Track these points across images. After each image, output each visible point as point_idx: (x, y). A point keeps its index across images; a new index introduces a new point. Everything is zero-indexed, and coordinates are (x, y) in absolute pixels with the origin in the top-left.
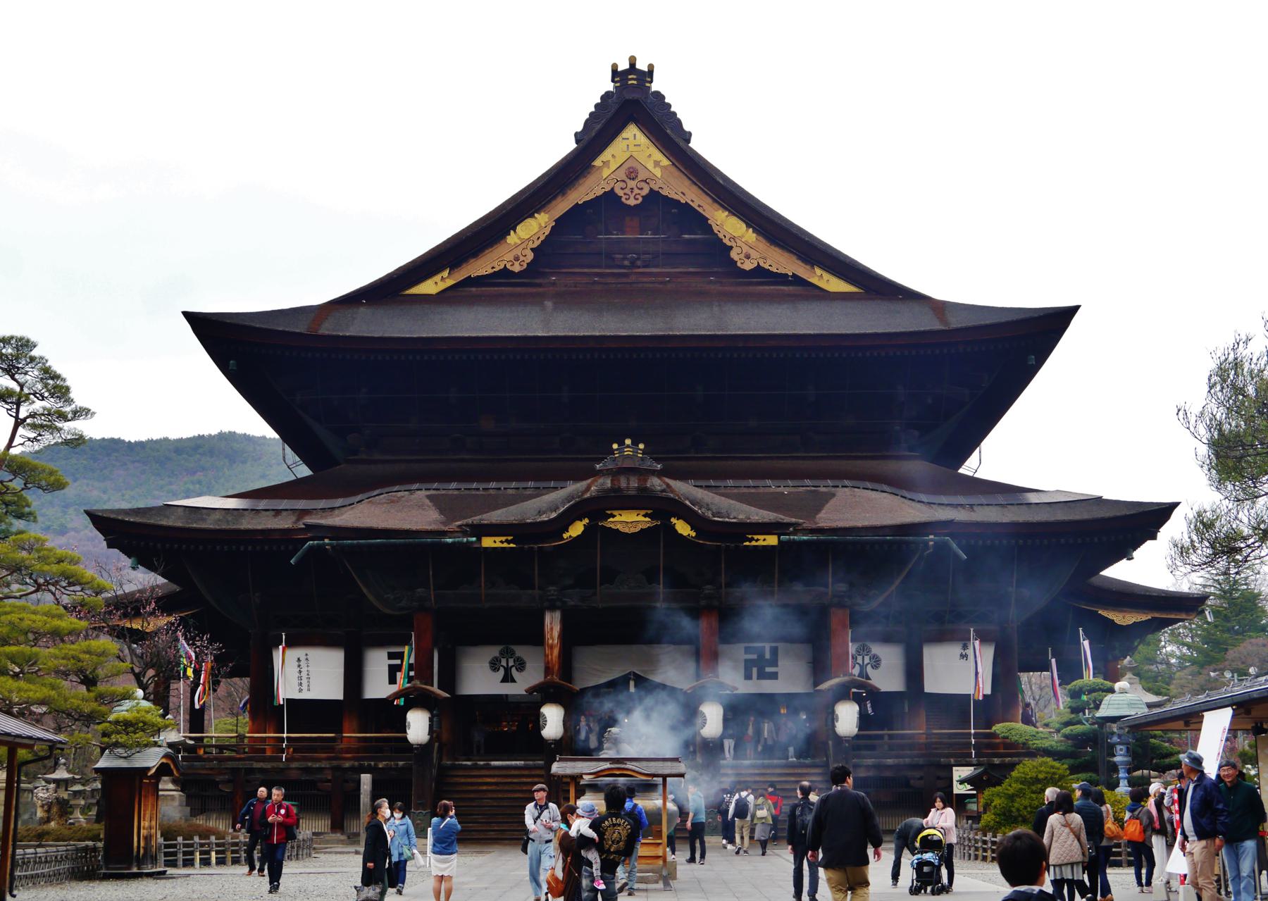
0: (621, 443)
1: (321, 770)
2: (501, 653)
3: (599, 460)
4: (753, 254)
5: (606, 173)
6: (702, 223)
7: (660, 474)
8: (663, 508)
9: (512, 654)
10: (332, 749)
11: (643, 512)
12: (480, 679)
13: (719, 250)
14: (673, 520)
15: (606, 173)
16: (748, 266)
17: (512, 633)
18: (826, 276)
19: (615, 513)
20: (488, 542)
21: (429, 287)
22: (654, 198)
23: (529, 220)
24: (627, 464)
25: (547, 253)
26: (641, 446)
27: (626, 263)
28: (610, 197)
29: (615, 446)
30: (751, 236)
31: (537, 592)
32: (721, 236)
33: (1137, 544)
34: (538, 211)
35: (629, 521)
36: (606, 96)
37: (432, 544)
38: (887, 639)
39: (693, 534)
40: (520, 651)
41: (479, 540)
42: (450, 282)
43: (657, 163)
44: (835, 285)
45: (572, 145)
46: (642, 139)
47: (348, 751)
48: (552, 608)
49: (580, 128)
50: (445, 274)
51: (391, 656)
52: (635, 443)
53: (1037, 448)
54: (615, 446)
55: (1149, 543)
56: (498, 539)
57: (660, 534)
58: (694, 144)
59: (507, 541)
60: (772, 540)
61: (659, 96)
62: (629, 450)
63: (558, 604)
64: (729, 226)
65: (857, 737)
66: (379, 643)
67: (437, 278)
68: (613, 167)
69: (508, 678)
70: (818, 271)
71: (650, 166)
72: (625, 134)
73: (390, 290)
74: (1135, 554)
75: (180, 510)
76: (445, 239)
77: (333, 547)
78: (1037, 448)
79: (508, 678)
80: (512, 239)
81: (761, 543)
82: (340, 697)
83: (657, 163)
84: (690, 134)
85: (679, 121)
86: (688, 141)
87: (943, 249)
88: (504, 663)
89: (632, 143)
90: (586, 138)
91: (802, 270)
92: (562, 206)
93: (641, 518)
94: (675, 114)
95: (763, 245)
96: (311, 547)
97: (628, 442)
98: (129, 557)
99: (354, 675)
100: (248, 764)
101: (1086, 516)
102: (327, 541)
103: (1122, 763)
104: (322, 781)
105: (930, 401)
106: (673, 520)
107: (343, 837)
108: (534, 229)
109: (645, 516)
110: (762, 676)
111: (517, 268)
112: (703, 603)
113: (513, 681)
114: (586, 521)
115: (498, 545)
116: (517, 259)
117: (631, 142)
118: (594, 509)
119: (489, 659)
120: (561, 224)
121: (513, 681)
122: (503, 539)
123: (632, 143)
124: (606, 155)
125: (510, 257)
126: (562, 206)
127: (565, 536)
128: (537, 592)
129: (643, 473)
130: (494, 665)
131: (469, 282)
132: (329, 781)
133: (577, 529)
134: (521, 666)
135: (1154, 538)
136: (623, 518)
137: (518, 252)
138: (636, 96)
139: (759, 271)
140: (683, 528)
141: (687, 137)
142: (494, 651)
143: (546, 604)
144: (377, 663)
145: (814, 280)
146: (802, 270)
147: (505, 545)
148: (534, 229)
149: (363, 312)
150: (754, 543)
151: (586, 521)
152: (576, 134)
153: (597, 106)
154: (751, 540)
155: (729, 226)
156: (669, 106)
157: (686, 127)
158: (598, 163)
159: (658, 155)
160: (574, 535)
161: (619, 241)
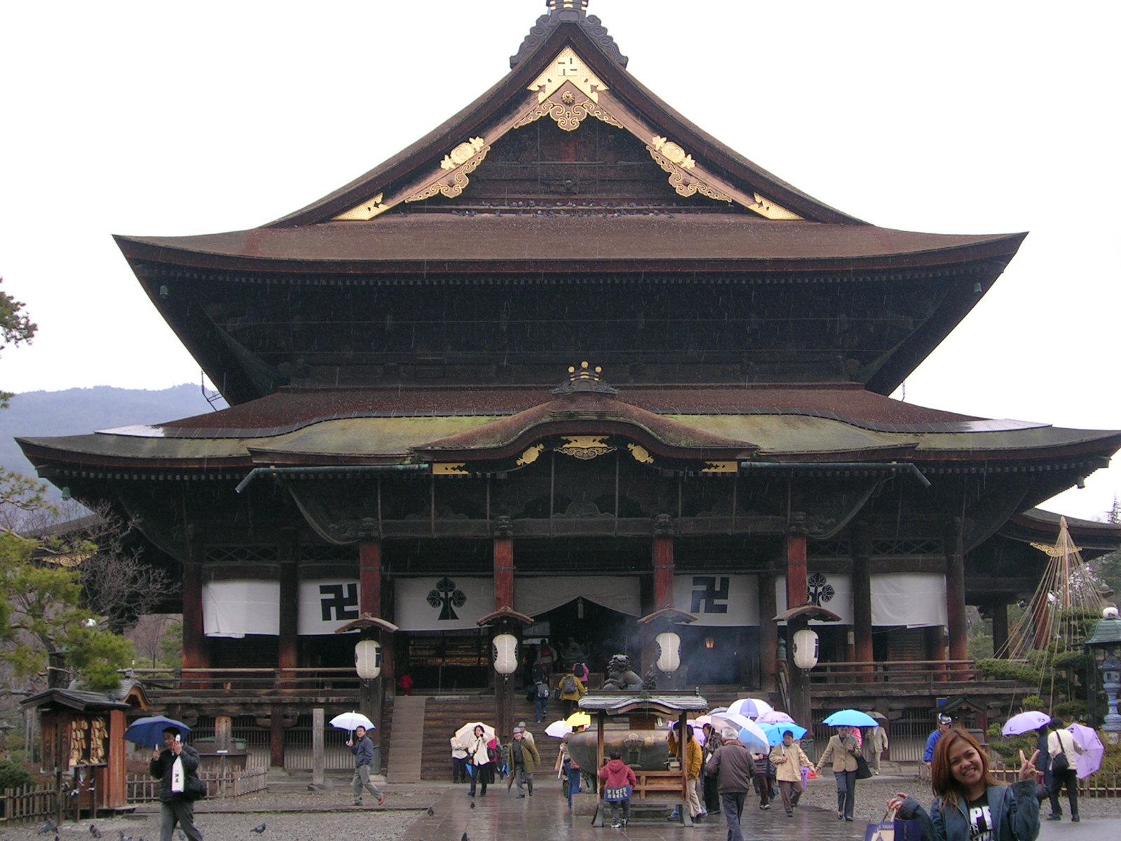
0: (578, 367)
1: (260, 705)
2: (440, 586)
4: (692, 180)
6: (641, 149)
8: (621, 435)
9: (452, 586)
11: (599, 438)
12: (418, 615)
13: (657, 176)
14: (630, 446)
15: (541, 97)
16: (686, 192)
17: (456, 562)
18: (766, 203)
19: (570, 438)
20: (439, 470)
21: (363, 213)
22: (590, 123)
23: (464, 146)
24: (584, 388)
25: (482, 182)
26: (598, 369)
28: (547, 122)
29: (571, 370)
30: (689, 163)
31: (488, 521)
32: (659, 162)
33: (1088, 471)
35: (584, 446)
36: (542, 20)
37: (382, 472)
38: (834, 572)
39: (651, 461)
40: (461, 584)
42: (383, 208)
43: (594, 88)
44: (775, 213)
45: (504, 70)
46: (578, 63)
47: (285, 686)
48: (504, 537)
49: (515, 52)
50: (379, 199)
52: (592, 367)
53: (972, 379)
55: (1100, 472)
56: (450, 466)
57: (618, 458)
58: (631, 69)
59: (460, 469)
60: (731, 467)
61: (594, 19)
62: (584, 375)
63: (510, 533)
64: (669, 153)
65: (815, 669)
66: (313, 576)
67: (371, 203)
68: (549, 92)
69: (447, 614)
70: (758, 199)
71: (586, 89)
72: (560, 58)
73: (324, 213)
74: (1088, 481)
75: (111, 439)
76: (402, 148)
77: (279, 474)
78: (972, 379)
79: (447, 614)
80: (446, 164)
81: (719, 470)
82: (277, 633)
83: (594, 88)
84: (627, 58)
85: (616, 45)
86: (625, 66)
87: (885, 180)
88: (442, 595)
89: (568, 69)
90: (521, 63)
91: (742, 199)
94: (611, 38)
95: (701, 173)
96: (257, 474)
97: (585, 365)
98: (61, 487)
99: (290, 610)
100: (185, 699)
102: (272, 468)
103: (1113, 690)
104: (260, 717)
106: (630, 446)
107: (284, 774)
108: (468, 153)
109: (601, 442)
110: (710, 609)
111: (452, 193)
112: (659, 531)
113: (454, 617)
114: (541, 446)
117: (568, 67)
118: (549, 436)
119: (426, 594)
120: (496, 149)
121: (454, 617)
122: (455, 465)
123: (568, 69)
124: (541, 80)
125: (445, 181)
127: (519, 463)
128: (488, 521)
129: (601, 396)
130: (433, 599)
131: (404, 208)
132: (268, 717)
133: (531, 456)
134: (460, 599)
135: (1105, 465)
136: (578, 445)
137: (455, 178)
138: (572, 18)
139: (700, 202)
140: (640, 455)
141: (624, 62)
142: (430, 585)
143: (497, 533)
144: (312, 597)
145: (754, 208)
146: (742, 199)
147: (457, 472)
148: (468, 153)
149: (295, 234)
150: (713, 470)
151: (541, 446)
152: (511, 58)
153: (532, 30)
154: (711, 466)
155: (669, 153)
156: (605, 30)
157: (623, 52)
159: (595, 81)
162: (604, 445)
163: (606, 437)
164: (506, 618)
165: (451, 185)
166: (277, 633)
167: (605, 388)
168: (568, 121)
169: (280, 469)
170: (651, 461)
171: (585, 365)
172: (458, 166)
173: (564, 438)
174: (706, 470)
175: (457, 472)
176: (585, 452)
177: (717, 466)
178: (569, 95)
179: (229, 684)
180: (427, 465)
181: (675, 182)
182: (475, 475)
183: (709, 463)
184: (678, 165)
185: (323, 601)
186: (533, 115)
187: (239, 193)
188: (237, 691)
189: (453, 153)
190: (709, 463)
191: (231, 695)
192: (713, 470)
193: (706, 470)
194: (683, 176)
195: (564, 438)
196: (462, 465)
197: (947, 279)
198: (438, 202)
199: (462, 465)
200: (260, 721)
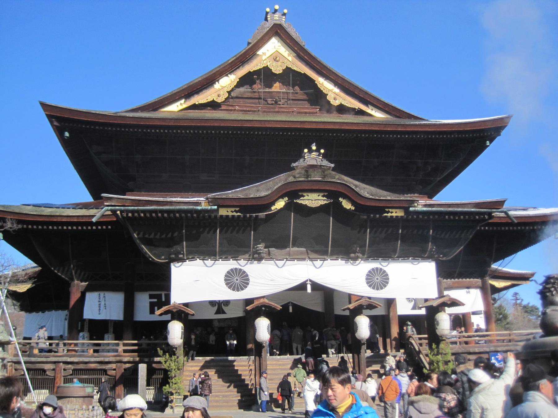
0: (311, 151)
3: (294, 163)
5: (264, 58)
7: (334, 169)
10: (117, 351)
11: (322, 194)
14: (341, 199)
16: (336, 103)
19: (305, 194)
20: (223, 212)
21: (175, 108)
22: (288, 71)
26: (322, 151)
27: (273, 102)
28: (266, 70)
29: (306, 151)
32: (322, 89)
34: (230, 73)
35: (313, 200)
39: (353, 208)
41: (217, 210)
42: (185, 106)
44: (378, 115)
50: (183, 101)
51: (151, 297)
52: (318, 150)
54: (306, 151)
56: (230, 210)
59: (237, 212)
67: (178, 103)
68: (268, 54)
80: (217, 86)
81: (394, 214)
92: (242, 72)
93: (320, 198)
95: (343, 95)
97: (314, 148)
101: (523, 221)
105: (429, 169)
106: (341, 199)
108: (227, 82)
111: (219, 100)
114: (286, 199)
115: (230, 214)
116: (219, 96)
122: (233, 209)
125: (216, 94)
126: (242, 72)
127: (273, 208)
131: (194, 107)
132: (115, 370)
133: (280, 204)
136: (309, 198)
137: (222, 93)
138: (278, 22)
140: (347, 205)
144: (143, 301)
147: (235, 214)
148: (227, 82)
150: (389, 215)
154: (388, 212)
158: (260, 52)
160: (279, 208)
161: (269, 92)
162: (325, 198)
163: (326, 194)
164: (265, 306)
165: (219, 96)
166: (121, 318)
167: (325, 163)
168: (277, 69)
169: (122, 208)
170: (353, 208)
171: (314, 148)
172: (223, 88)
173: (300, 194)
174: (386, 214)
175: (235, 214)
176: (313, 202)
177: (392, 212)
178: (276, 58)
179: (92, 350)
180: (216, 207)
181: (330, 98)
182: (245, 216)
183: (387, 210)
184: (331, 91)
185: (151, 303)
186: (260, 66)
187: (111, 98)
188: (96, 354)
189: (221, 81)
190: (387, 210)
191: (92, 356)
192: (389, 215)
193: (386, 214)
194: (333, 96)
195: (300, 194)
196: (237, 209)
197: (466, 144)
198: (213, 105)
199: (237, 209)
200: (109, 373)
